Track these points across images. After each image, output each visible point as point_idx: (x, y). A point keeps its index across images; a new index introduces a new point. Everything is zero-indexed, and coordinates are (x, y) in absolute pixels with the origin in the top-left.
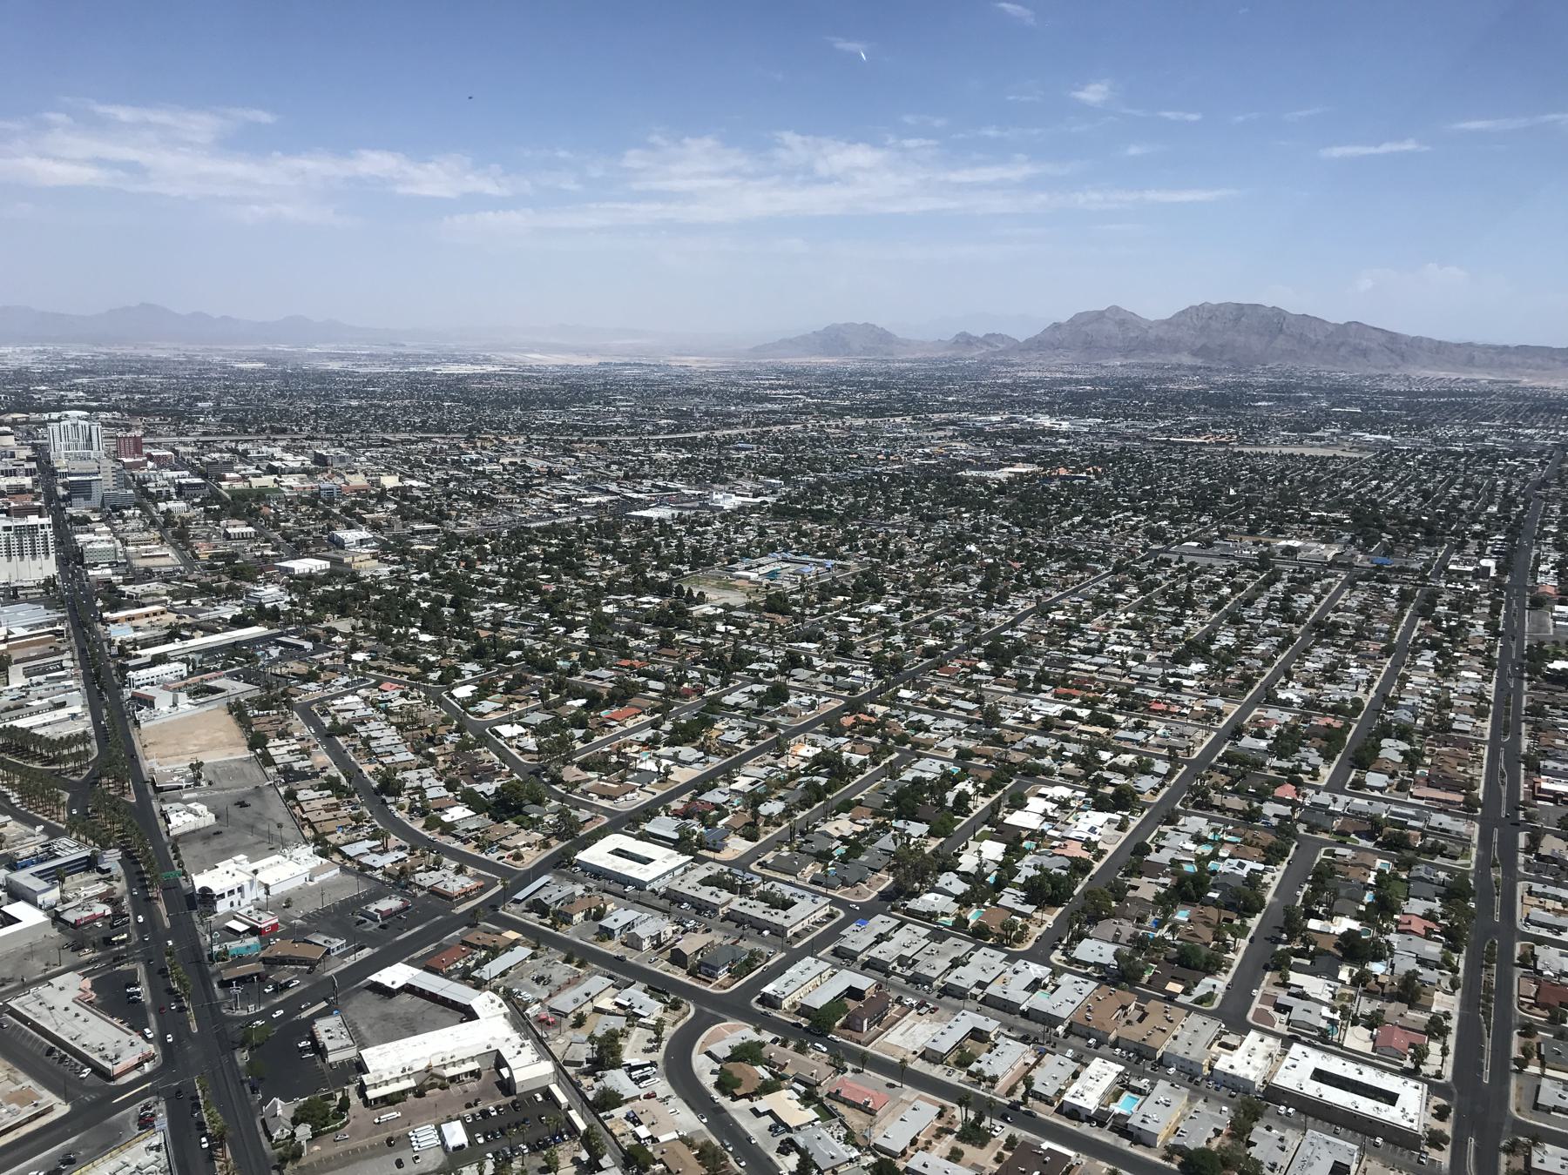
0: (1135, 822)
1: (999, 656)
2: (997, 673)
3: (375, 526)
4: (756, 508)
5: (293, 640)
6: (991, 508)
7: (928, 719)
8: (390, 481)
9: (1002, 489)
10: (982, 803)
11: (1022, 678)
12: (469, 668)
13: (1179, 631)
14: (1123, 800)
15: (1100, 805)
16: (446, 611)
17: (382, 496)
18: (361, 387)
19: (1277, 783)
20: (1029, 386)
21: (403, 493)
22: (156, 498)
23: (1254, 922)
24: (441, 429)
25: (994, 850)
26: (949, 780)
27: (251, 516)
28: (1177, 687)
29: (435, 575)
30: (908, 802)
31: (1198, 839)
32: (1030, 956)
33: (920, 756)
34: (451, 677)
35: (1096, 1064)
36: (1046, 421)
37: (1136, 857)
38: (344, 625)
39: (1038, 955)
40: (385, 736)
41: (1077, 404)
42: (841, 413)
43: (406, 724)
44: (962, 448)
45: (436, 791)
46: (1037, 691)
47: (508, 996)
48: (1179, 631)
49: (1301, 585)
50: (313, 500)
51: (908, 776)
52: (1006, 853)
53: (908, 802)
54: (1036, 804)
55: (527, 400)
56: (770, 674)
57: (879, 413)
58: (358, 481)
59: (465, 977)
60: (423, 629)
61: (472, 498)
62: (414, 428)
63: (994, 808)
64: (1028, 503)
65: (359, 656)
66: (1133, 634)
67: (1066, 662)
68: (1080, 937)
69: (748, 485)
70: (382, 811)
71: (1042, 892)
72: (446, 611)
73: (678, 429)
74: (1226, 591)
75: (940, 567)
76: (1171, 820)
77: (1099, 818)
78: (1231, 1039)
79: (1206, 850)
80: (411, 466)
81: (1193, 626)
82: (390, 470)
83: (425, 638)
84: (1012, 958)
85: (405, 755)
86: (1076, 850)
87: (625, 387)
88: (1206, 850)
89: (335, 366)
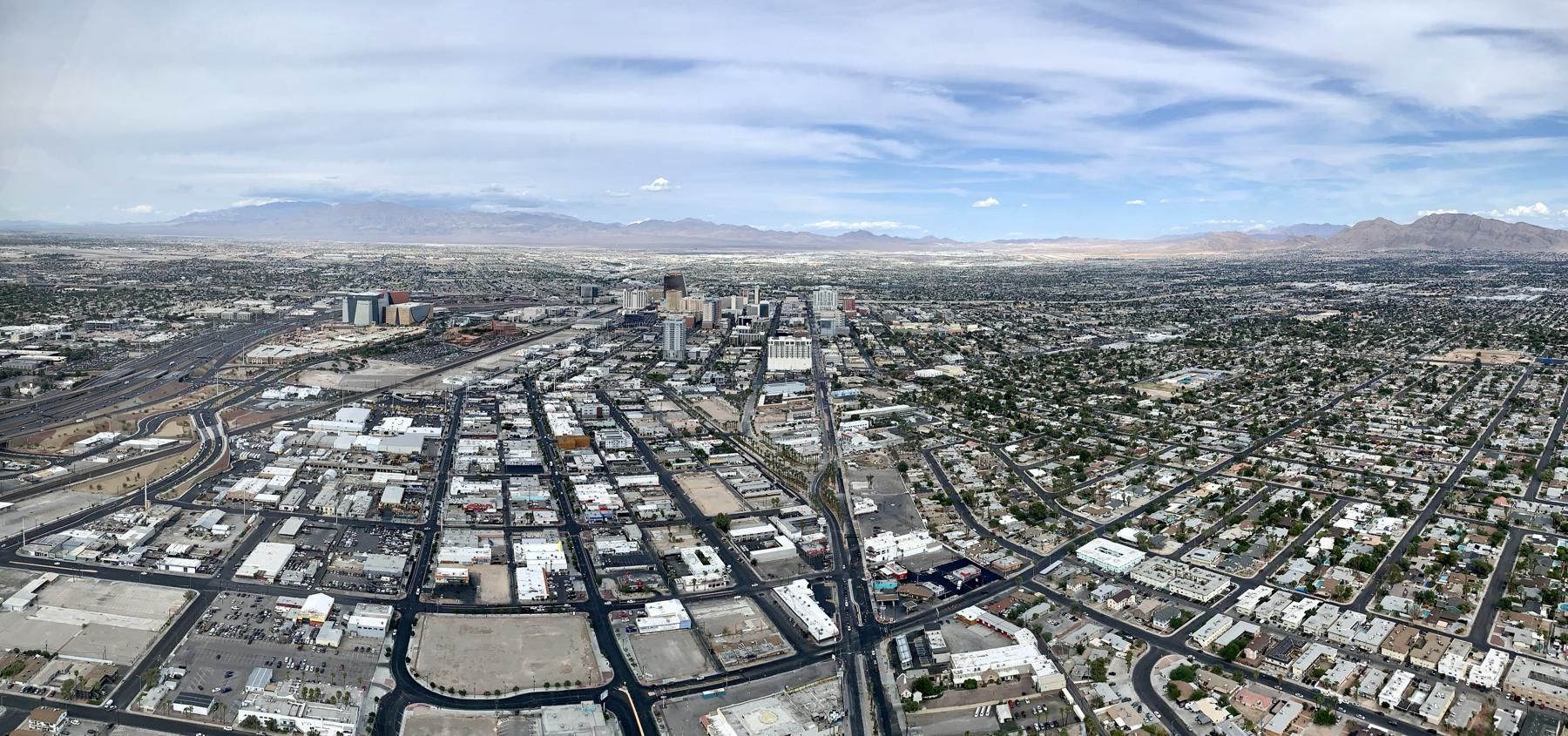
0: (1411, 523)
1: (1324, 425)
2: (1324, 434)
3: (965, 353)
4: (1173, 342)
5: (923, 413)
6: (1314, 337)
7: (1284, 465)
8: (972, 328)
9: (1320, 326)
10: (1320, 514)
11: (1339, 438)
12: (1015, 435)
13: (1430, 406)
14: (1404, 509)
15: (1391, 514)
16: (1003, 401)
17: (969, 335)
18: (958, 276)
19: (1495, 496)
20: (1332, 266)
21: (979, 335)
22: (859, 332)
23: (1487, 581)
24: (1001, 298)
25: (1328, 543)
26: (1299, 501)
27: (904, 344)
28: (1431, 440)
29: (997, 380)
30: (1273, 516)
31: (1450, 532)
32: (1352, 608)
33: (1280, 488)
34: (1003, 439)
35: (1397, 674)
36: (1341, 285)
37: (1413, 544)
38: (948, 407)
39: (1359, 606)
40: (969, 471)
41: (1361, 275)
42: (1223, 283)
43: (981, 467)
44: (1296, 303)
45: (996, 506)
46: (1348, 445)
47: (1037, 631)
48: (1430, 406)
49: (1498, 378)
50: (935, 336)
51: (1273, 500)
52: (1336, 543)
53: (1273, 516)
54: (1351, 514)
55: (1047, 282)
56: (1187, 439)
57: (1245, 283)
58: (956, 327)
59: (1012, 618)
60: (990, 411)
61: (1017, 337)
62: (987, 298)
63: (1327, 516)
64: (1335, 333)
65: (955, 425)
66: (1402, 409)
67: (1364, 428)
68: (1384, 594)
69: (1170, 328)
70: (967, 516)
71: (1360, 565)
72: (1003, 401)
73: (1130, 296)
74: (1456, 382)
75: (1286, 372)
76: (1434, 520)
77: (1390, 521)
78: (1479, 655)
79: (1455, 538)
80: (984, 319)
81: (1437, 403)
82: (973, 322)
83: (991, 416)
84: (1342, 609)
85: (979, 484)
86: (1377, 541)
87: (1096, 272)
88: (1455, 538)
89: (946, 264)
